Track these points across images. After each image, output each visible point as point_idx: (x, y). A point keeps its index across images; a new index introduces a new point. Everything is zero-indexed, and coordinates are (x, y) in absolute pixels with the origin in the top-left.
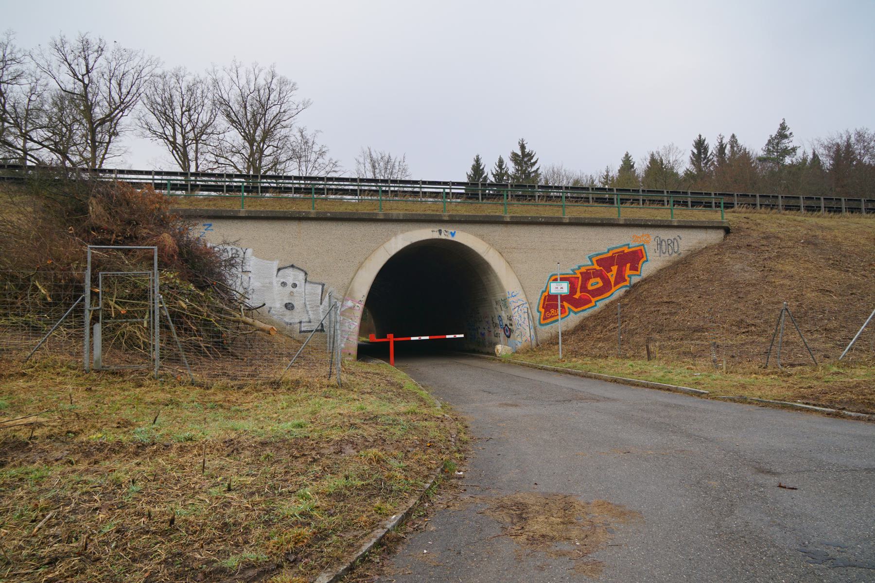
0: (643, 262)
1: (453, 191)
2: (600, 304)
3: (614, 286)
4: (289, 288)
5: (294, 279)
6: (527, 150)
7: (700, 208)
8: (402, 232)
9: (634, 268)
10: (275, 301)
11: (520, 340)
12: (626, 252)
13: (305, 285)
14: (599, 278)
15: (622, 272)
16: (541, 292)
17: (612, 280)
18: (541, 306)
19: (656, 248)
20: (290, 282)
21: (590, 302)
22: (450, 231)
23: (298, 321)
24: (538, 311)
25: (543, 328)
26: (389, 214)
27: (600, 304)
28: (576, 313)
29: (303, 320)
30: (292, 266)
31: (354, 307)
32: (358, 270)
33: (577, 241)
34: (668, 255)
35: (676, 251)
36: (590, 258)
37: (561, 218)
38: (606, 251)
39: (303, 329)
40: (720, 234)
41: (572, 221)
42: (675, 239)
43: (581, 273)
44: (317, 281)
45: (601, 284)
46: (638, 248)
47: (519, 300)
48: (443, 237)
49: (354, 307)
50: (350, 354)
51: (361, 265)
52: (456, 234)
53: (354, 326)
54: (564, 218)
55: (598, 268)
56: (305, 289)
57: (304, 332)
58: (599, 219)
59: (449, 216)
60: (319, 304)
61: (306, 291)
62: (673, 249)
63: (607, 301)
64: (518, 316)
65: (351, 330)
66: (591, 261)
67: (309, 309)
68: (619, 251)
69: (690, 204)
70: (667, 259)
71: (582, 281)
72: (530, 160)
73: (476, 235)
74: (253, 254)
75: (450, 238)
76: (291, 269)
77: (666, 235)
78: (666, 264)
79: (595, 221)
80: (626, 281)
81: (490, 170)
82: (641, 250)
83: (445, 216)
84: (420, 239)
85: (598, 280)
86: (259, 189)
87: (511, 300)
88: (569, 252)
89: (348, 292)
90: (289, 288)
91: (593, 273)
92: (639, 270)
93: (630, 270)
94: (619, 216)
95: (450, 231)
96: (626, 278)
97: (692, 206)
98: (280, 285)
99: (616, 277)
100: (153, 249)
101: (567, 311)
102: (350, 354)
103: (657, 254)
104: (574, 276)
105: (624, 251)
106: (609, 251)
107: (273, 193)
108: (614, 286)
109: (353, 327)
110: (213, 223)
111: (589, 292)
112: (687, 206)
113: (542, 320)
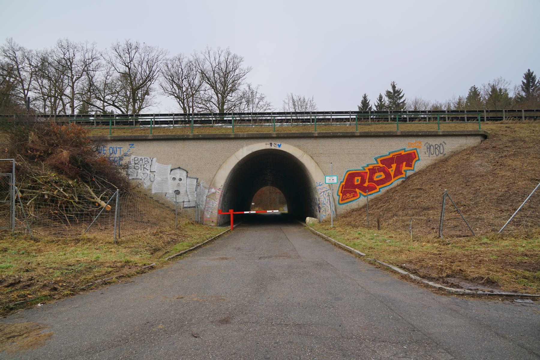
0: (416, 161)
1: (333, 117)
2: (383, 190)
3: (394, 178)
4: (177, 181)
6: (396, 89)
7: (474, 122)
8: (247, 145)
9: (409, 165)
10: (169, 189)
11: (324, 214)
12: (402, 154)
13: (186, 179)
14: (382, 173)
15: (399, 168)
16: (340, 182)
17: (392, 174)
18: (340, 191)
19: (426, 151)
20: (178, 177)
21: (376, 188)
22: (278, 144)
23: (182, 201)
24: (338, 195)
25: (341, 206)
26: (238, 134)
27: (383, 190)
28: (365, 196)
29: (185, 201)
30: (179, 168)
31: (216, 192)
32: (218, 170)
33: (366, 147)
34: (435, 156)
35: (441, 152)
36: (376, 159)
37: (354, 133)
38: (388, 154)
39: (185, 206)
40: (478, 140)
41: (362, 134)
42: (441, 144)
43: (369, 169)
44: (193, 177)
45: (359, 178)
46: (412, 151)
47: (324, 188)
48: (273, 147)
49: (216, 192)
50: (213, 222)
51: (220, 167)
52: (281, 145)
53: (216, 204)
54: (356, 133)
55: (381, 165)
57: (186, 207)
58: (382, 132)
59: (276, 134)
60: (195, 191)
61: (187, 182)
62: (439, 151)
63: (388, 188)
64: (323, 198)
65: (214, 207)
67: (189, 194)
68: (397, 153)
69: (466, 119)
70: (435, 158)
71: (370, 175)
72: (399, 95)
73: (295, 146)
74: (157, 161)
75: (278, 148)
76: (178, 170)
77: (433, 141)
78: (433, 162)
79: (379, 134)
80: (402, 174)
81: (373, 103)
82: (414, 153)
83: (274, 134)
84: (256, 150)
85: (382, 173)
86: (173, 122)
87: (318, 188)
88: (361, 156)
89: (212, 183)
90: (177, 181)
91: (378, 169)
92: (413, 166)
93: (406, 166)
94: (398, 130)
95: (278, 144)
96: (403, 172)
97: (468, 120)
98: (172, 179)
99: (395, 171)
100: (12, 160)
101: (359, 195)
102: (213, 222)
103: (427, 155)
104: (363, 171)
105: (401, 154)
106: (390, 154)
107: (181, 124)
108: (394, 178)
109: (215, 205)
110: (134, 144)
111: (375, 182)
112: (464, 120)
113: (340, 201)
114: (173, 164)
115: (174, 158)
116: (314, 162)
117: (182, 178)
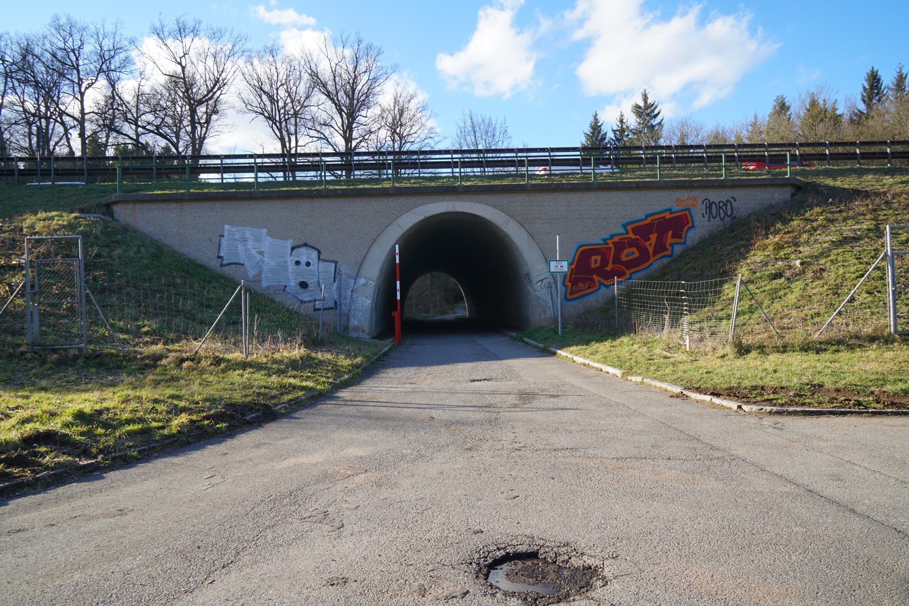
0: (689, 228)
3: (653, 256)
5: (308, 258)
6: (649, 101)
9: (677, 235)
12: (667, 217)
17: (651, 250)
18: (567, 279)
19: (704, 212)
20: (303, 260)
21: (625, 274)
25: (570, 303)
30: (306, 245)
34: (719, 220)
35: (729, 214)
39: (317, 307)
42: (728, 201)
43: (614, 243)
44: (330, 259)
55: (633, 237)
56: (318, 268)
60: (332, 282)
61: (320, 269)
66: (626, 230)
68: (659, 217)
72: (653, 111)
73: (494, 206)
74: (268, 234)
80: (667, 250)
81: (609, 129)
82: (686, 215)
85: (634, 250)
92: (683, 237)
93: (673, 237)
96: (668, 246)
98: (294, 264)
101: (597, 283)
104: (605, 246)
105: (665, 217)
106: (647, 217)
108: (653, 256)
111: (623, 263)
114: (295, 239)
115: (296, 228)
116: (526, 233)
117: (310, 261)
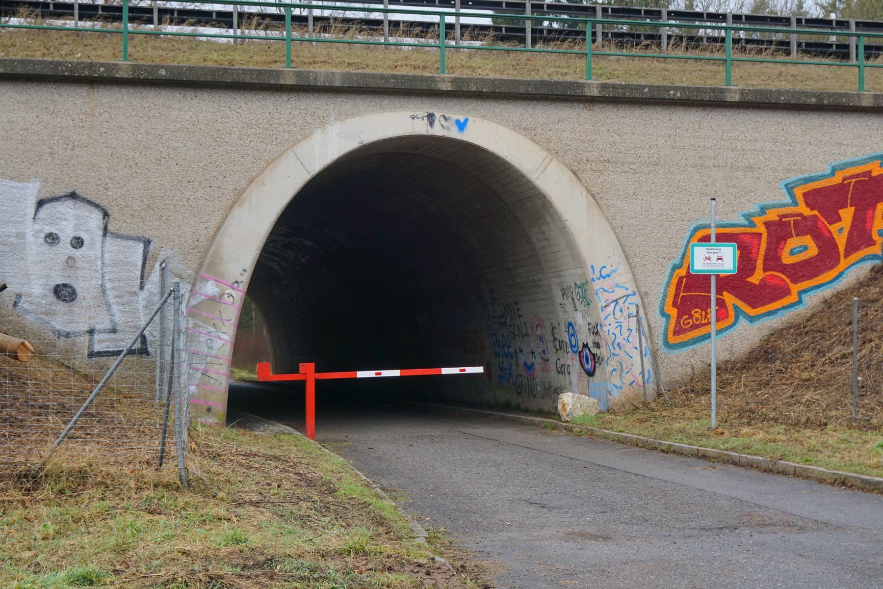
1: (464, 20)
3: (846, 256)
4: (64, 249)
5: (77, 227)
8: (340, 117)
11: (617, 382)
12: (874, 174)
13: (103, 243)
14: (809, 236)
15: (864, 221)
17: (841, 242)
18: (670, 300)
20: (67, 232)
21: (788, 292)
23: (87, 328)
24: (663, 313)
25: (675, 353)
26: (308, 72)
28: (752, 319)
29: (98, 327)
30: (73, 196)
32: (231, 207)
33: (758, 146)
36: (790, 189)
37: (722, 91)
38: (828, 171)
39: (97, 348)
41: (750, 98)
43: (767, 224)
44: (132, 233)
47: (617, 286)
48: (437, 131)
50: (209, 410)
51: (238, 197)
52: (469, 124)
53: (221, 343)
54: (730, 91)
55: (807, 212)
56: (103, 252)
57: (100, 354)
58: (813, 95)
59: (454, 81)
60: (136, 288)
61: (106, 255)
63: (827, 292)
64: (614, 325)
65: (214, 353)
66: (792, 195)
67: (112, 300)
71: (769, 243)
75: (454, 133)
76: (70, 203)
79: (803, 100)
83: (443, 80)
85: (808, 240)
87: (597, 285)
88: (740, 174)
89: (207, 261)
90: (64, 249)
91: (796, 223)
94: (861, 88)
95: (455, 117)
96: (875, 237)
98: (42, 240)
99: (850, 234)
102: (209, 410)
104: (749, 230)
105: (870, 172)
106: (834, 171)
107: (28, 16)
108: (846, 256)
109: (218, 344)
111: (784, 269)
113: (670, 336)
114: (46, 181)
115: (51, 154)
116: (585, 192)
117: (84, 236)
